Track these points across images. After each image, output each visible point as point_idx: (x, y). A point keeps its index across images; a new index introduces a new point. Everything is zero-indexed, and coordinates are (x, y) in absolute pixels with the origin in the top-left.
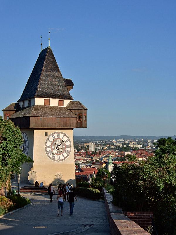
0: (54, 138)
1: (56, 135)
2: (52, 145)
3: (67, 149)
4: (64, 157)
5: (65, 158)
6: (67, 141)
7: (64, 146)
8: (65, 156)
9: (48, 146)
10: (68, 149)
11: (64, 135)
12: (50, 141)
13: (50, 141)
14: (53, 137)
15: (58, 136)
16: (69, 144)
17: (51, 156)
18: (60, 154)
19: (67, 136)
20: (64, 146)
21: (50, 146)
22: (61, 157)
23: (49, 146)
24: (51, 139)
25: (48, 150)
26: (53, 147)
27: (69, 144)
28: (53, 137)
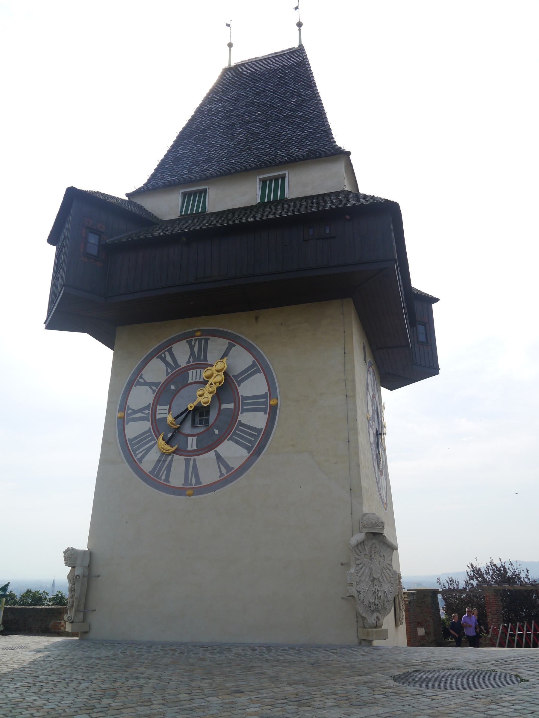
1: (182, 353)
2: (157, 401)
3: (245, 418)
4: (227, 466)
5: (231, 475)
6: (248, 373)
7: (231, 406)
8: (235, 465)
9: (135, 412)
10: (257, 420)
12: (150, 385)
13: (150, 385)
14: (168, 358)
15: (192, 354)
16: (263, 389)
17: (148, 463)
18: (202, 449)
19: (249, 348)
20: (231, 406)
21: (147, 408)
22: (207, 468)
23: (141, 410)
24: (157, 371)
25: (134, 429)
26: (162, 412)
27: (263, 389)
28: (168, 358)
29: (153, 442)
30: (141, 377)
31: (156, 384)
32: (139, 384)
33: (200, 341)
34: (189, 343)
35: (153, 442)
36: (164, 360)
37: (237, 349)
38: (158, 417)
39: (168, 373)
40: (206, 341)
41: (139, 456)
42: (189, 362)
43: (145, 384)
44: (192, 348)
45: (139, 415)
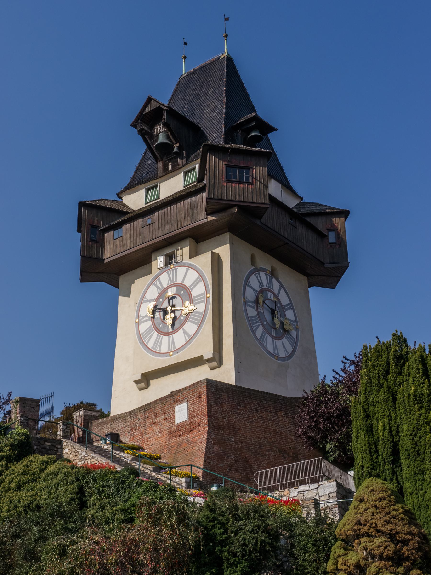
0: (261, 284)
11: (282, 286)
12: (254, 290)
13: (254, 290)
29: (259, 324)
30: (249, 282)
31: (257, 291)
32: (248, 286)
33: (270, 276)
34: (266, 274)
35: (259, 324)
36: (257, 278)
37: (282, 290)
38: (259, 310)
39: (260, 288)
40: (272, 278)
41: (255, 328)
42: (266, 286)
43: (251, 287)
44: (267, 278)
45: (251, 304)
